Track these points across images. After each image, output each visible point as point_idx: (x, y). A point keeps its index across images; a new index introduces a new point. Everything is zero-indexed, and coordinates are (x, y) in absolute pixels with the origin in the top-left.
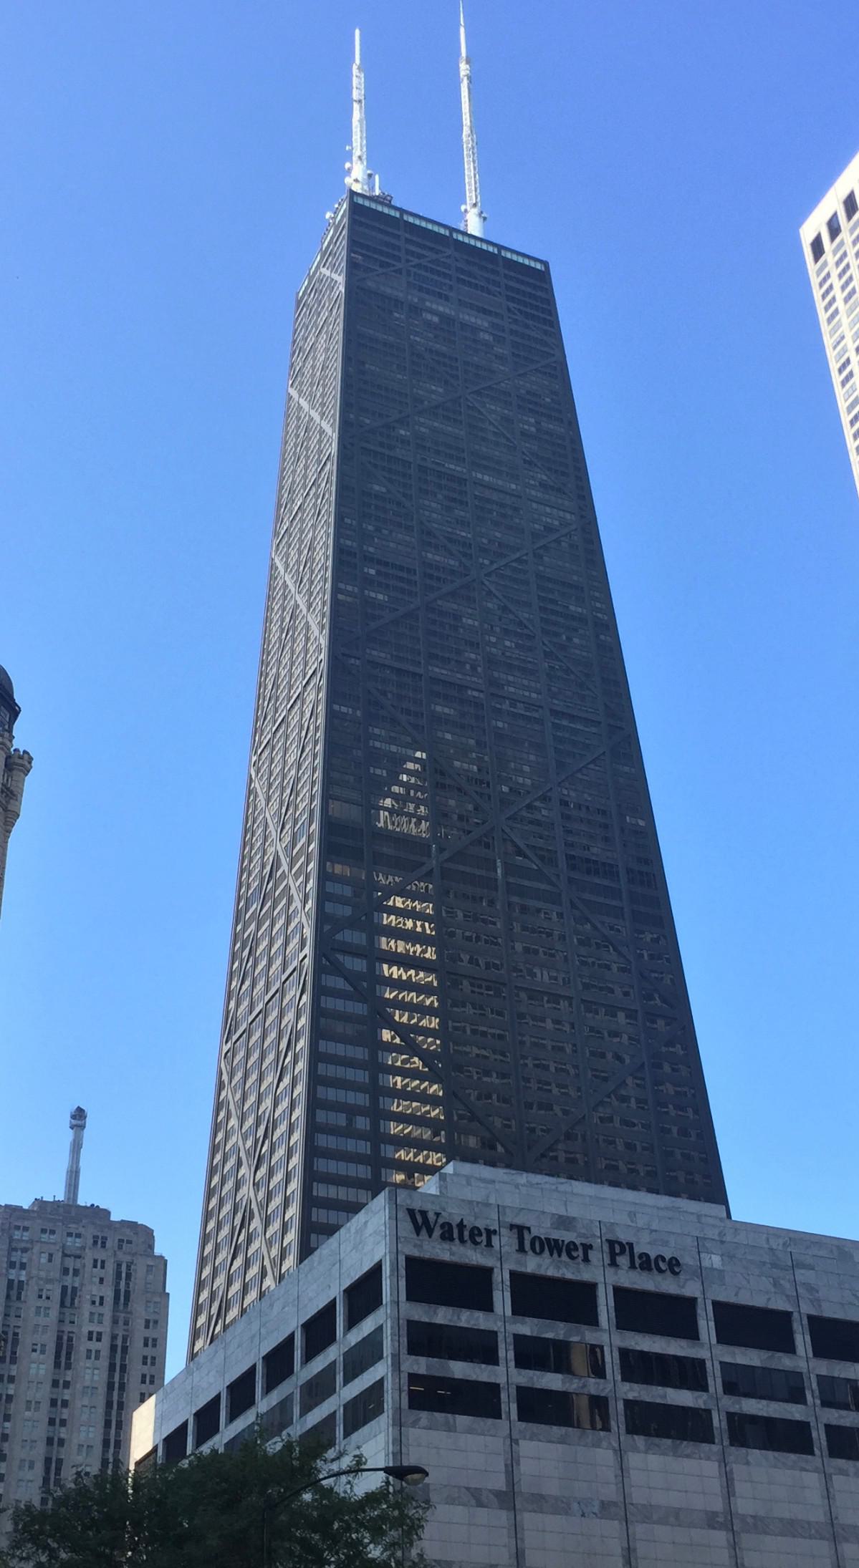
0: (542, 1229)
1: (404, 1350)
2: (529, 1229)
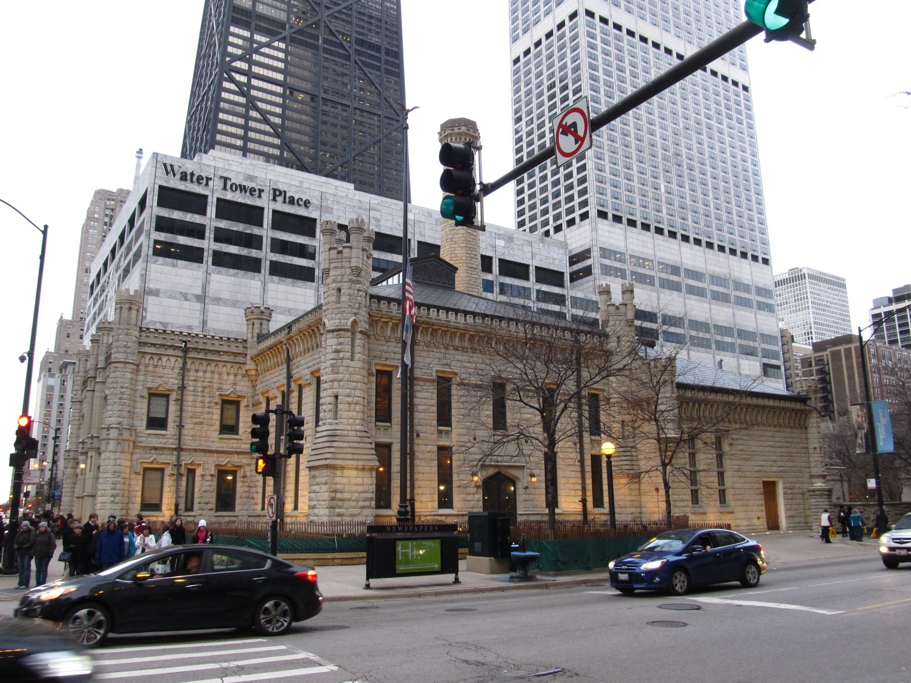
0: (237, 180)
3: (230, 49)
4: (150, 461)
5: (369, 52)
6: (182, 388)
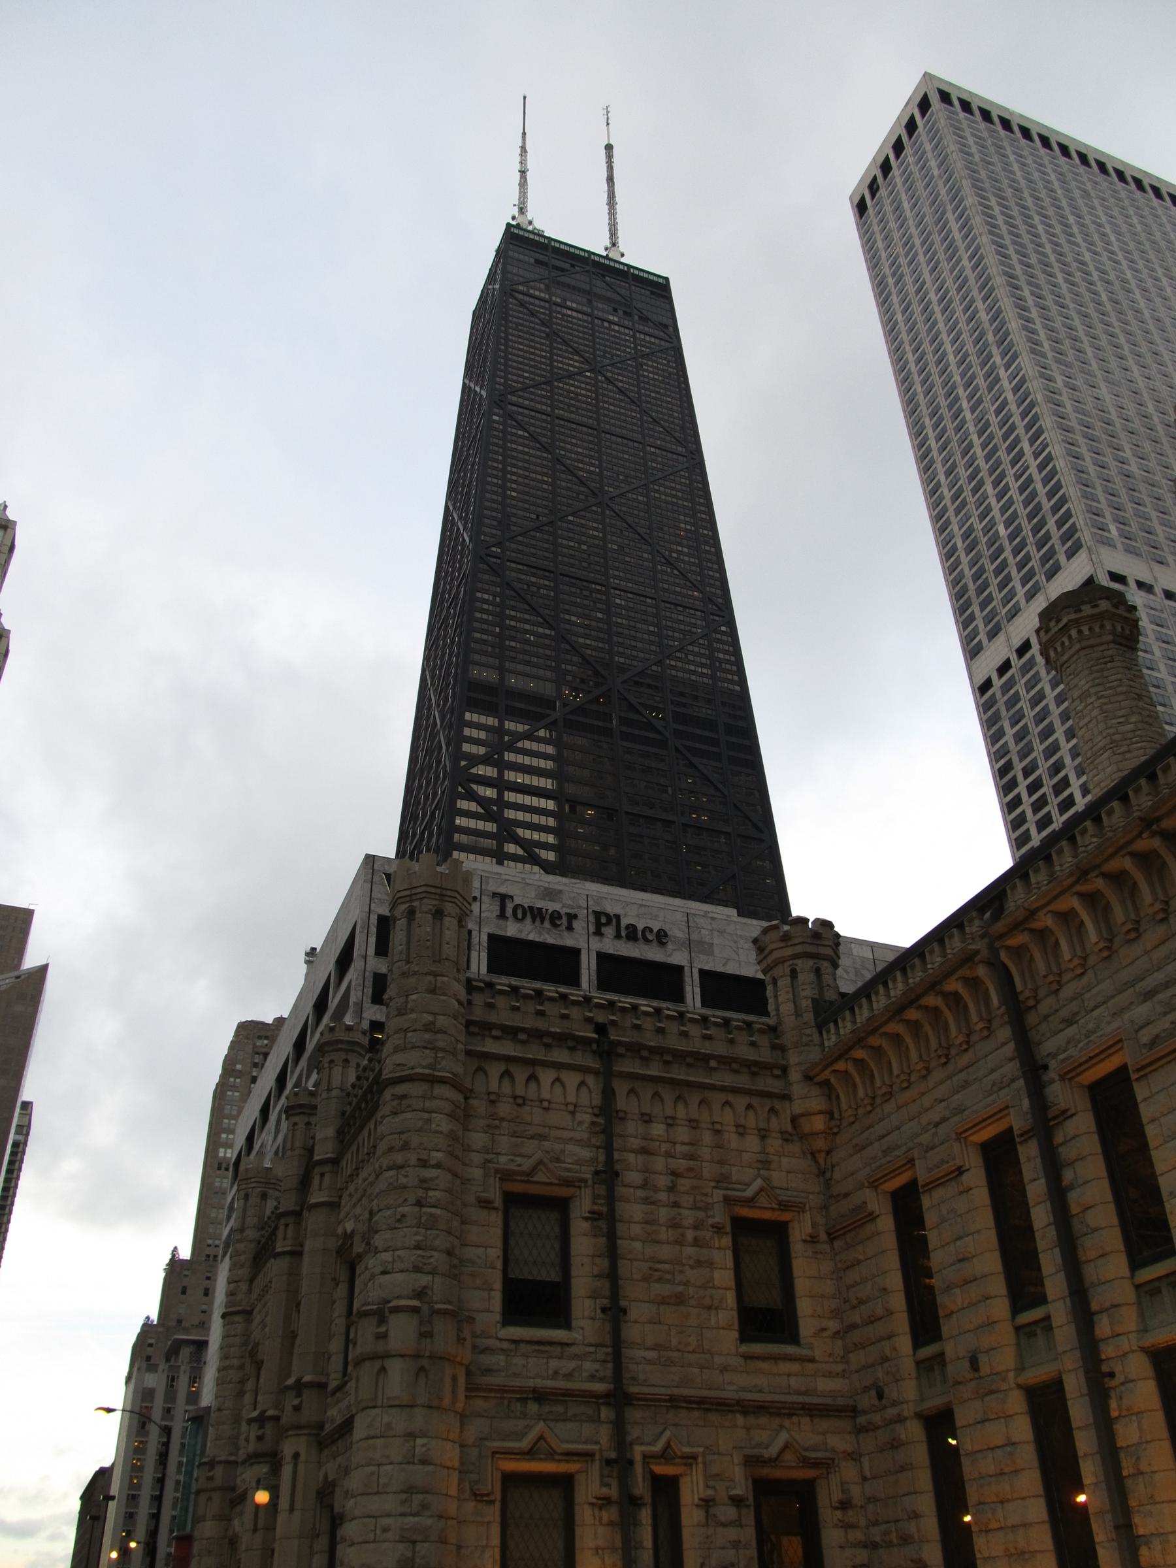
0: (524, 897)
1: (367, 1000)
2: (512, 897)
3: (466, 747)
4: (525, 1444)
5: (698, 732)
6: (609, 1175)
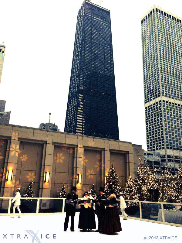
3: (79, 100)
